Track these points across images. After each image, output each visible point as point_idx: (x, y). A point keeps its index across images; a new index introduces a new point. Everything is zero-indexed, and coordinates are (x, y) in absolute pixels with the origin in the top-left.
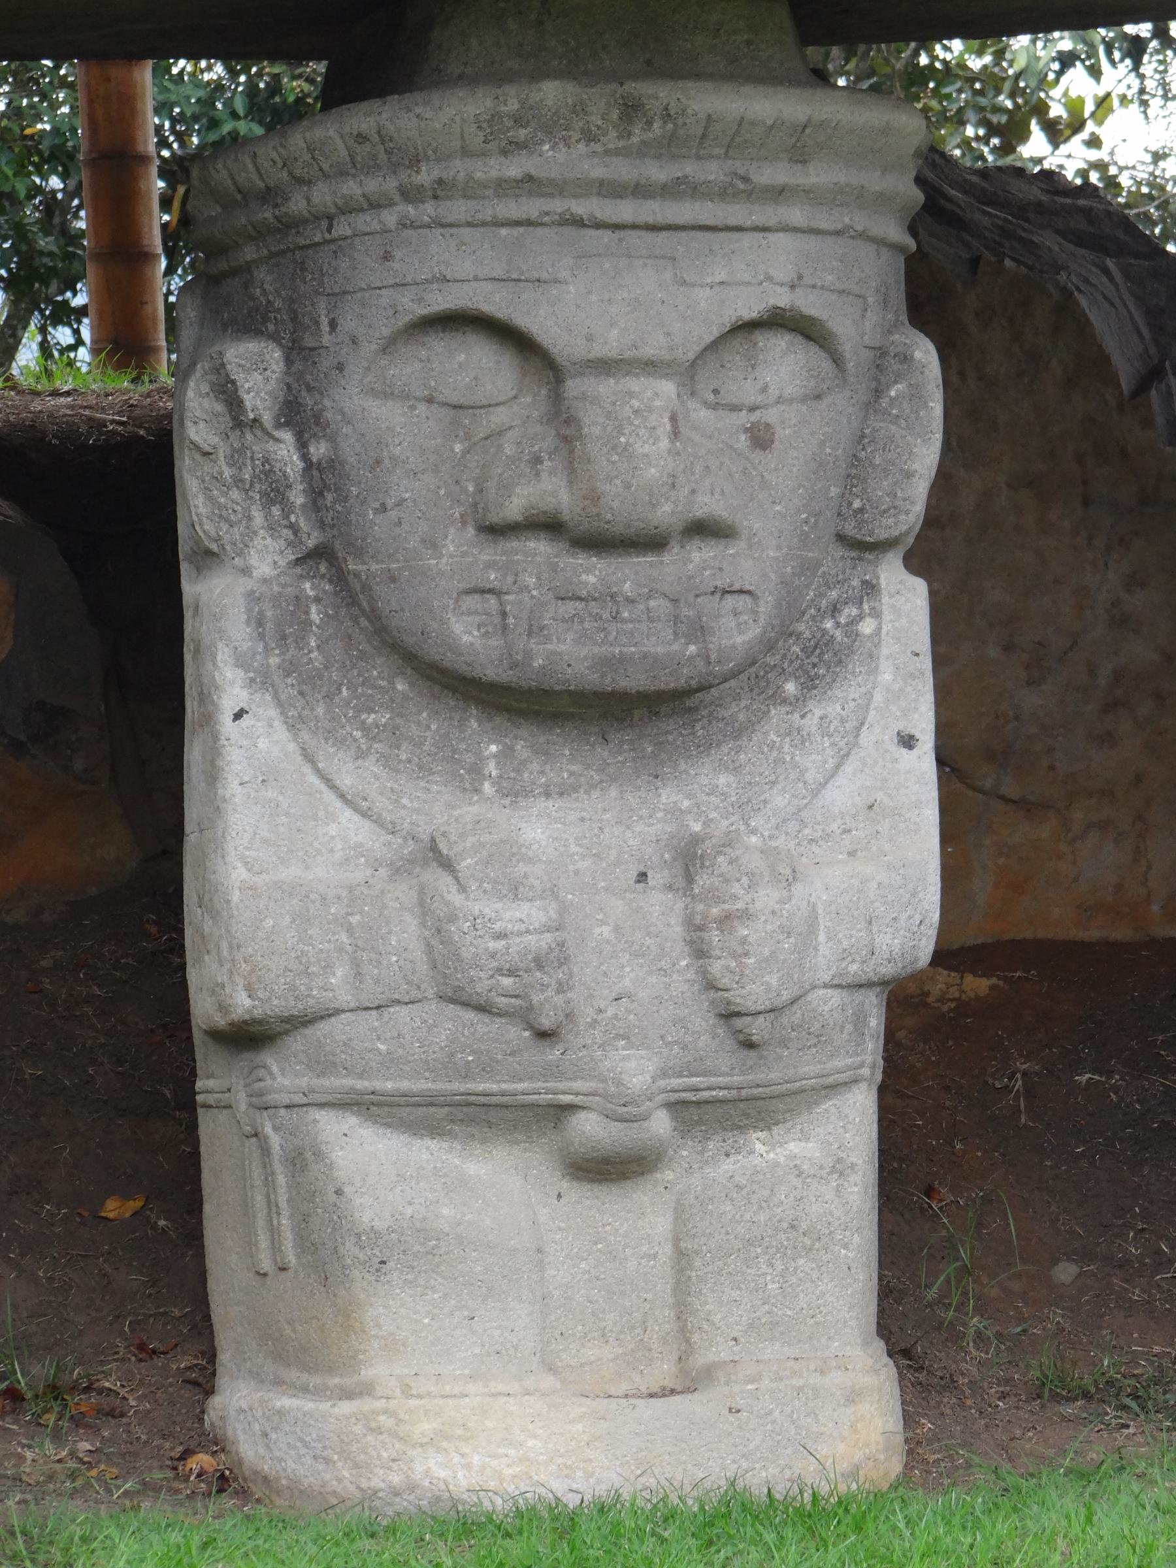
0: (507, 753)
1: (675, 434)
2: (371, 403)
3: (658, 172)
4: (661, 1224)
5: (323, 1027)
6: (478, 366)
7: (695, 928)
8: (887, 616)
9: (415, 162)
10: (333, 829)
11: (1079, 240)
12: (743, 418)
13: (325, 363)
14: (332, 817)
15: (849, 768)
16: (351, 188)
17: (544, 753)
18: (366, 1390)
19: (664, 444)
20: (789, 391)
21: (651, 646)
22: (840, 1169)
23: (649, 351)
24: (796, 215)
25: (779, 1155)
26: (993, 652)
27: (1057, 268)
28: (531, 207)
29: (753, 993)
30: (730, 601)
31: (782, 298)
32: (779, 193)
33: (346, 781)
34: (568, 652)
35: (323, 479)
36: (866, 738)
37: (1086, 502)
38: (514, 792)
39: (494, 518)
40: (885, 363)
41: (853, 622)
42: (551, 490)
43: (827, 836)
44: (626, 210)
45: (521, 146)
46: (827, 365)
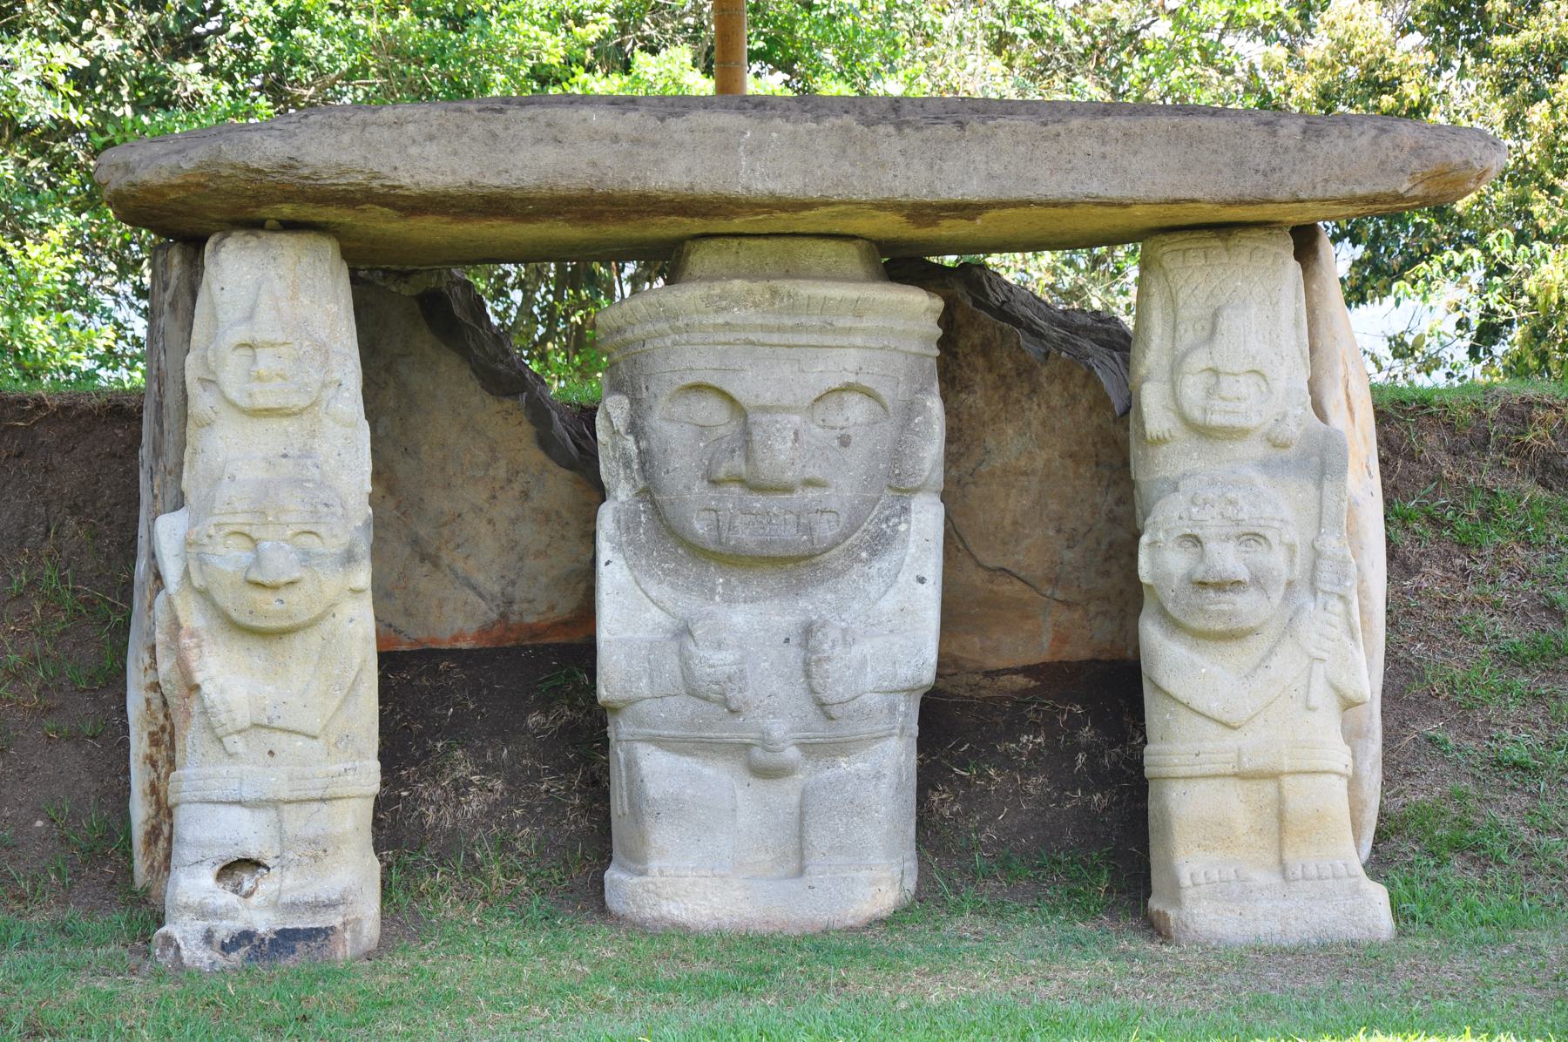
0: (727, 583)
1: (796, 440)
2: (664, 424)
3: (788, 321)
4: (794, 799)
5: (639, 705)
6: (710, 410)
7: (806, 663)
8: (914, 522)
9: (676, 317)
10: (648, 616)
11: (1102, 344)
12: (837, 432)
13: (645, 406)
14: (648, 610)
15: (892, 591)
16: (650, 327)
17: (745, 583)
18: (643, 873)
19: (789, 444)
20: (860, 420)
21: (788, 533)
22: (878, 776)
23: (785, 402)
24: (859, 341)
25: (852, 769)
26: (1051, 533)
27: (1088, 356)
28: (731, 337)
29: (830, 695)
30: (825, 516)
31: (852, 379)
32: (849, 331)
33: (653, 594)
34: (744, 535)
35: (645, 457)
36: (901, 578)
37: (1097, 465)
38: (729, 600)
39: (714, 477)
40: (910, 410)
41: (896, 525)
42: (738, 465)
43: (880, 623)
44: (775, 338)
45: (724, 309)
46: (879, 408)
